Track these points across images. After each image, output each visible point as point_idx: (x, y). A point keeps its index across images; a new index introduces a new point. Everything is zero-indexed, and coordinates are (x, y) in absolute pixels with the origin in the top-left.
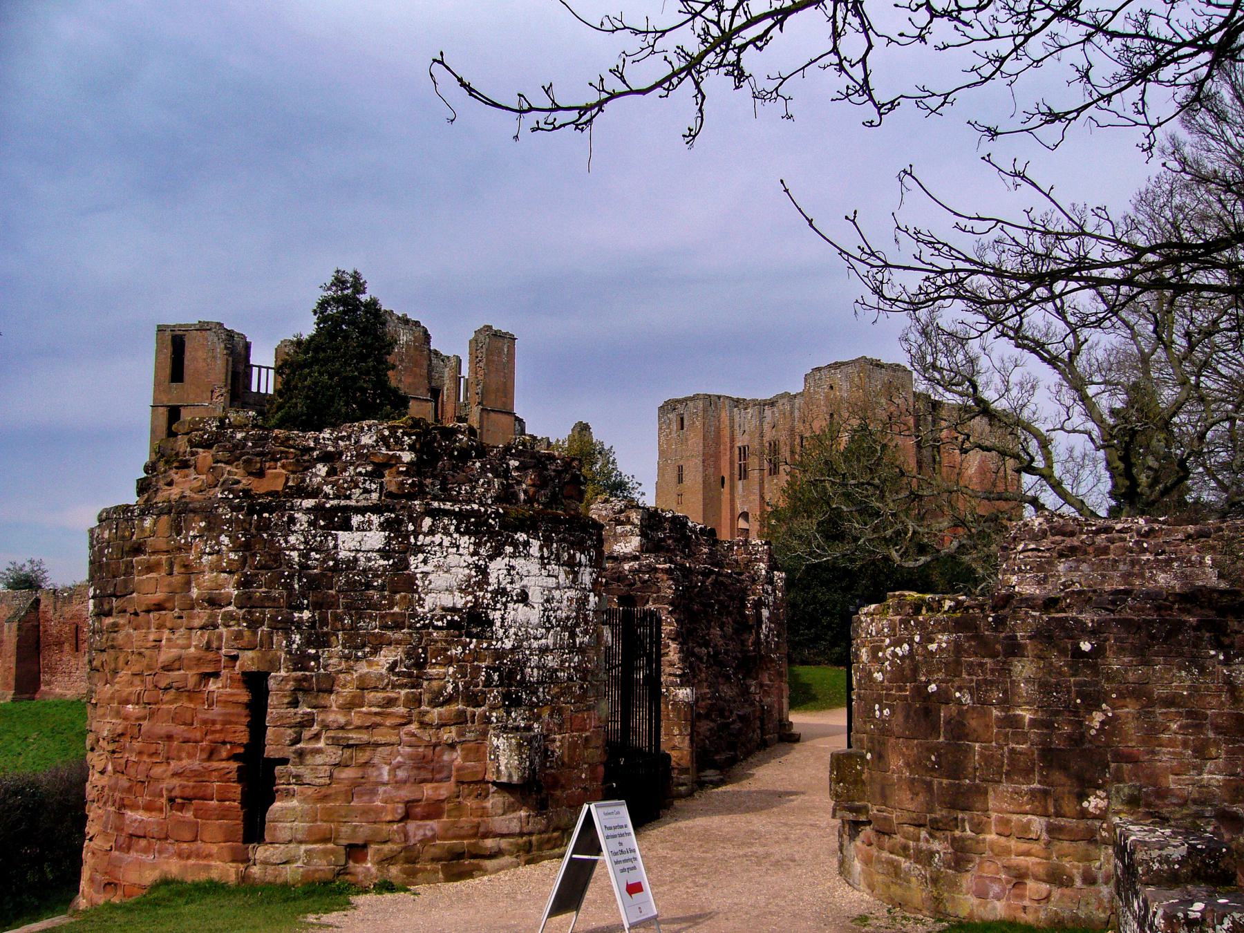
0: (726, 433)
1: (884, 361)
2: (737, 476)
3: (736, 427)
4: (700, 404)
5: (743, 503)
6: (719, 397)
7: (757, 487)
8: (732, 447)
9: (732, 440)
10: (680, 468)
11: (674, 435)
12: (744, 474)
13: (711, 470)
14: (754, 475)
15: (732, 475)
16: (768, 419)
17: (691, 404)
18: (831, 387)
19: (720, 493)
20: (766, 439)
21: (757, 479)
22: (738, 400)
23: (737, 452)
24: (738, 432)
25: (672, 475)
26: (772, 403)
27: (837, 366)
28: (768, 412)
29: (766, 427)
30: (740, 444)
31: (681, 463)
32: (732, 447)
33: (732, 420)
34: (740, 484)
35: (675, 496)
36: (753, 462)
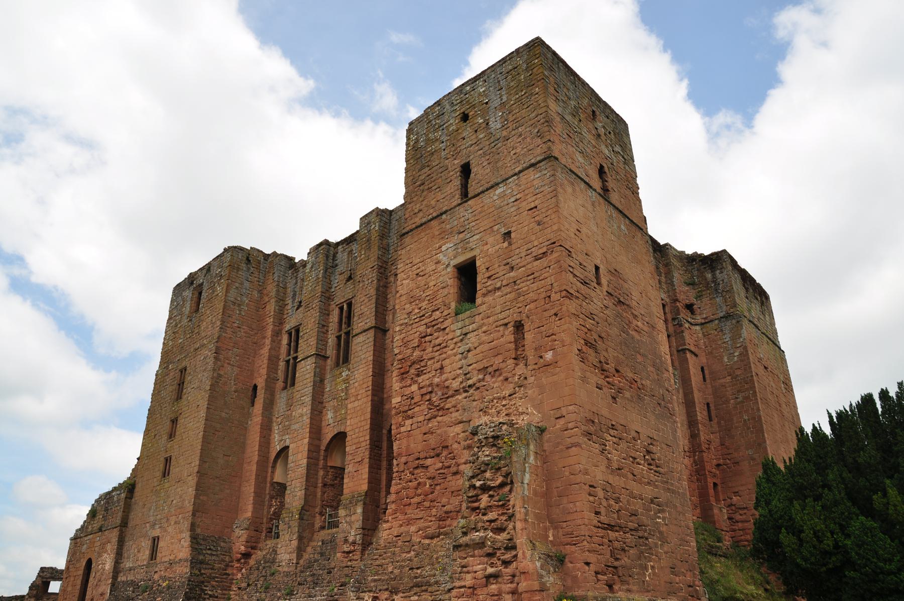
2: (280, 384)
9: (280, 320)
11: (185, 321)
12: (290, 380)
14: (306, 370)
15: (271, 381)
16: (340, 268)
18: (465, 118)
19: (248, 415)
23: (285, 340)
28: (342, 256)
29: (338, 280)
30: (287, 327)
31: (183, 365)
32: (277, 334)
34: (281, 399)
36: (308, 346)
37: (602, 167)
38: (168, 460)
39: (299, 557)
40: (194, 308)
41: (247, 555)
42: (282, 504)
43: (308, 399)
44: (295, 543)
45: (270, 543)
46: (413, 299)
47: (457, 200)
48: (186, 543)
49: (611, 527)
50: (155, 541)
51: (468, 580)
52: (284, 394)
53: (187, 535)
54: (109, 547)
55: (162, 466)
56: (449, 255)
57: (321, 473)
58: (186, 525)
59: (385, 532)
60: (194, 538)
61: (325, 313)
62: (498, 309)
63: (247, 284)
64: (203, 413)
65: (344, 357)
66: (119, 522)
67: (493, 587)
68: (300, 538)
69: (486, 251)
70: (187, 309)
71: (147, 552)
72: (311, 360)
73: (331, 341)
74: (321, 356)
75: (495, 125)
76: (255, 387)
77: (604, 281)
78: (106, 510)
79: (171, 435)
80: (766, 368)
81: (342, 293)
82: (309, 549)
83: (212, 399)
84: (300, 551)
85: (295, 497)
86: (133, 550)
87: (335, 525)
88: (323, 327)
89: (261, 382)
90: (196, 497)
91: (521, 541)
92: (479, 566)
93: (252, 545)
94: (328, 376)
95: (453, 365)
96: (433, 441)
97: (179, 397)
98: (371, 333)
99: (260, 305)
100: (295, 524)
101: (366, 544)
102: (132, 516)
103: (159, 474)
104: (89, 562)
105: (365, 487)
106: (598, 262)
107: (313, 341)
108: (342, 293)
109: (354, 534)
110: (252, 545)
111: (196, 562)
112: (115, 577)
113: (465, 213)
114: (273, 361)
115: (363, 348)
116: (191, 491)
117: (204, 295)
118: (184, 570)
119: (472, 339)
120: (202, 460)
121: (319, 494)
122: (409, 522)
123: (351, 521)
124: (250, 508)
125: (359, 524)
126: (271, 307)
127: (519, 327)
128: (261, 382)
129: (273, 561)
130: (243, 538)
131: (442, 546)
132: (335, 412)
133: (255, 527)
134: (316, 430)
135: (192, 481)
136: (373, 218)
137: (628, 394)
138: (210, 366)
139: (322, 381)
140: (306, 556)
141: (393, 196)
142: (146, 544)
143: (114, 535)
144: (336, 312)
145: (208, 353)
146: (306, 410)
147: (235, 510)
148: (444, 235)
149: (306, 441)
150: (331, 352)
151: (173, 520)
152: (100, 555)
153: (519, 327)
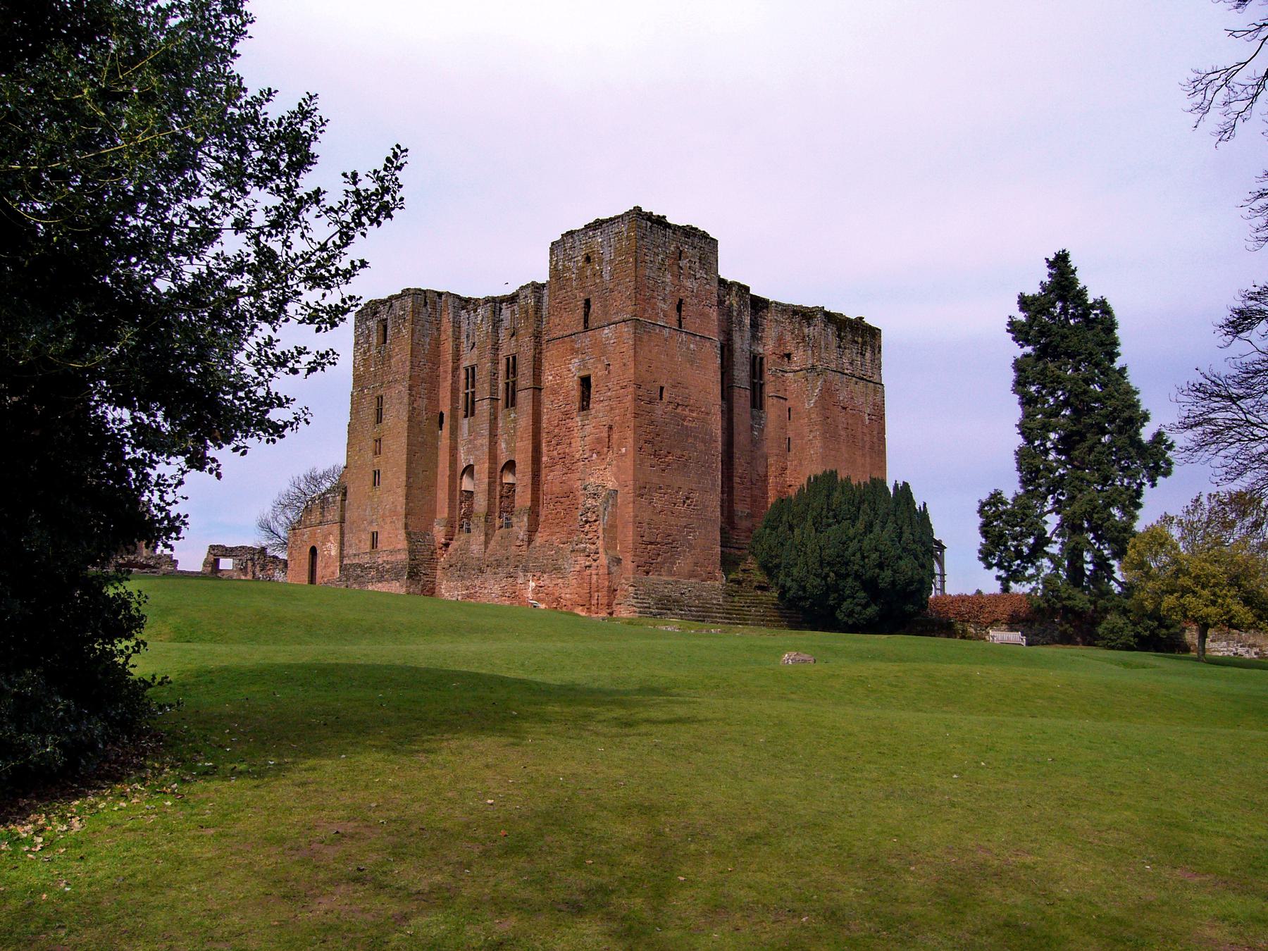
0: (448, 346)
1: (670, 220)
2: (461, 413)
3: (463, 338)
4: (409, 302)
5: (469, 452)
6: (440, 294)
7: (486, 426)
8: (455, 369)
9: (457, 357)
10: (380, 399)
11: (374, 352)
12: (470, 410)
13: (422, 403)
14: (483, 407)
15: (454, 410)
16: (506, 323)
17: (397, 304)
18: (588, 259)
19: (437, 438)
20: (502, 354)
21: (486, 415)
22: (468, 300)
23: (463, 376)
24: (464, 346)
25: (369, 413)
26: (512, 299)
27: (598, 224)
28: (506, 313)
29: (503, 334)
31: (380, 393)
32: (455, 369)
33: (457, 326)
34: (465, 424)
35: (371, 443)
36: (483, 389)
37: (681, 301)
38: (376, 473)
39: (486, 548)
40: (382, 340)
41: (447, 545)
42: (471, 506)
43: (486, 433)
44: (482, 538)
45: (464, 536)
46: (554, 392)
47: (581, 328)
48: (402, 534)
49: (651, 543)
50: (374, 537)
51: (578, 568)
52: (466, 421)
53: (403, 532)
54: (331, 538)
55: (372, 477)
56: (575, 368)
57: (498, 488)
58: (401, 524)
59: (539, 539)
60: (408, 534)
61: (495, 362)
62: (601, 415)
63: (427, 325)
64: (404, 440)
65: (511, 401)
66: (337, 519)
67: (588, 572)
68: (486, 535)
69: (597, 373)
70: (374, 339)
71: (369, 543)
72: (486, 402)
73: (501, 386)
74: (494, 400)
75: (606, 277)
76: (442, 415)
77: (665, 394)
78: (323, 508)
79: (377, 452)
80: (844, 408)
81: (507, 347)
82: (492, 543)
83: (410, 428)
84: (486, 543)
85: (481, 503)
86: (354, 541)
87: (509, 525)
88: (494, 374)
89: (446, 409)
90: (407, 504)
91: (601, 550)
92: (583, 561)
93: (450, 538)
94: (500, 415)
95: (577, 443)
96: (565, 487)
97: (379, 420)
98: (530, 391)
99: (437, 344)
100: (482, 525)
101: (530, 541)
102: (347, 515)
103: (370, 483)
104: (313, 551)
105: (529, 504)
106: (664, 384)
107: (487, 386)
108: (507, 347)
109: (522, 534)
110: (450, 538)
111: (411, 552)
112: (341, 561)
113: (586, 340)
114: (455, 391)
115: (524, 398)
116: (402, 500)
117: (389, 332)
118: (403, 557)
119: (588, 429)
120: (408, 478)
121: (497, 501)
122: (552, 534)
123: (521, 525)
124: (447, 510)
125: (525, 528)
126: (448, 346)
127: (610, 428)
128: (446, 409)
129: (467, 550)
130: (443, 533)
131: (568, 547)
132: (507, 444)
133: (450, 524)
134: (493, 457)
135: (401, 492)
136: (528, 291)
137: (675, 466)
138: (406, 400)
139: (496, 418)
140: (490, 547)
141: (543, 277)
142: (366, 538)
143: (336, 529)
144: (504, 361)
145: (403, 388)
146: (486, 441)
147: (434, 512)
148: (574, 351)
149: (487, 465)
150: (501, 395)
151: (388, 520)
152: (324, 544)
153: (610, 428)
